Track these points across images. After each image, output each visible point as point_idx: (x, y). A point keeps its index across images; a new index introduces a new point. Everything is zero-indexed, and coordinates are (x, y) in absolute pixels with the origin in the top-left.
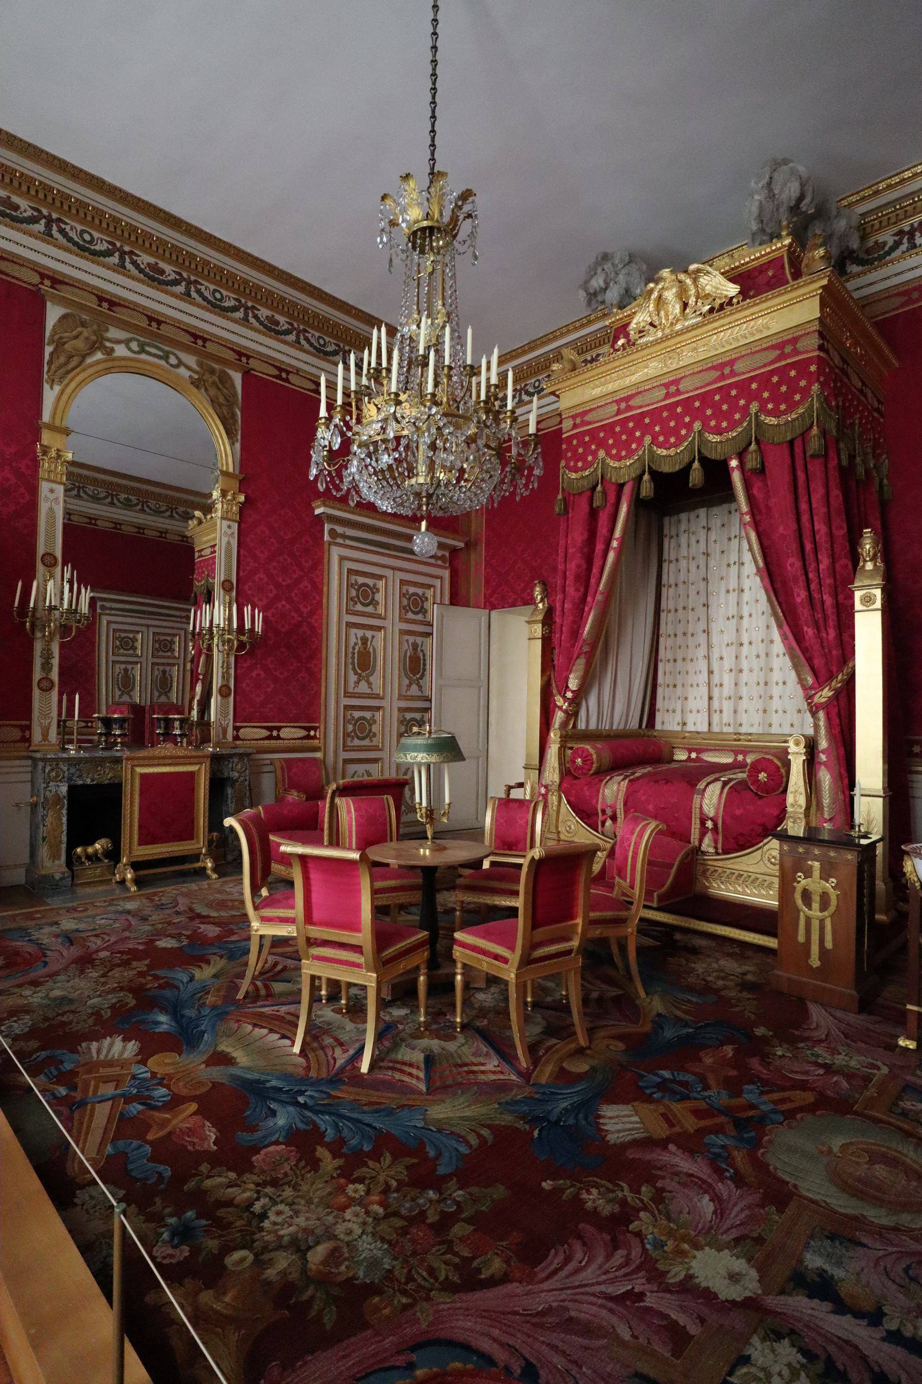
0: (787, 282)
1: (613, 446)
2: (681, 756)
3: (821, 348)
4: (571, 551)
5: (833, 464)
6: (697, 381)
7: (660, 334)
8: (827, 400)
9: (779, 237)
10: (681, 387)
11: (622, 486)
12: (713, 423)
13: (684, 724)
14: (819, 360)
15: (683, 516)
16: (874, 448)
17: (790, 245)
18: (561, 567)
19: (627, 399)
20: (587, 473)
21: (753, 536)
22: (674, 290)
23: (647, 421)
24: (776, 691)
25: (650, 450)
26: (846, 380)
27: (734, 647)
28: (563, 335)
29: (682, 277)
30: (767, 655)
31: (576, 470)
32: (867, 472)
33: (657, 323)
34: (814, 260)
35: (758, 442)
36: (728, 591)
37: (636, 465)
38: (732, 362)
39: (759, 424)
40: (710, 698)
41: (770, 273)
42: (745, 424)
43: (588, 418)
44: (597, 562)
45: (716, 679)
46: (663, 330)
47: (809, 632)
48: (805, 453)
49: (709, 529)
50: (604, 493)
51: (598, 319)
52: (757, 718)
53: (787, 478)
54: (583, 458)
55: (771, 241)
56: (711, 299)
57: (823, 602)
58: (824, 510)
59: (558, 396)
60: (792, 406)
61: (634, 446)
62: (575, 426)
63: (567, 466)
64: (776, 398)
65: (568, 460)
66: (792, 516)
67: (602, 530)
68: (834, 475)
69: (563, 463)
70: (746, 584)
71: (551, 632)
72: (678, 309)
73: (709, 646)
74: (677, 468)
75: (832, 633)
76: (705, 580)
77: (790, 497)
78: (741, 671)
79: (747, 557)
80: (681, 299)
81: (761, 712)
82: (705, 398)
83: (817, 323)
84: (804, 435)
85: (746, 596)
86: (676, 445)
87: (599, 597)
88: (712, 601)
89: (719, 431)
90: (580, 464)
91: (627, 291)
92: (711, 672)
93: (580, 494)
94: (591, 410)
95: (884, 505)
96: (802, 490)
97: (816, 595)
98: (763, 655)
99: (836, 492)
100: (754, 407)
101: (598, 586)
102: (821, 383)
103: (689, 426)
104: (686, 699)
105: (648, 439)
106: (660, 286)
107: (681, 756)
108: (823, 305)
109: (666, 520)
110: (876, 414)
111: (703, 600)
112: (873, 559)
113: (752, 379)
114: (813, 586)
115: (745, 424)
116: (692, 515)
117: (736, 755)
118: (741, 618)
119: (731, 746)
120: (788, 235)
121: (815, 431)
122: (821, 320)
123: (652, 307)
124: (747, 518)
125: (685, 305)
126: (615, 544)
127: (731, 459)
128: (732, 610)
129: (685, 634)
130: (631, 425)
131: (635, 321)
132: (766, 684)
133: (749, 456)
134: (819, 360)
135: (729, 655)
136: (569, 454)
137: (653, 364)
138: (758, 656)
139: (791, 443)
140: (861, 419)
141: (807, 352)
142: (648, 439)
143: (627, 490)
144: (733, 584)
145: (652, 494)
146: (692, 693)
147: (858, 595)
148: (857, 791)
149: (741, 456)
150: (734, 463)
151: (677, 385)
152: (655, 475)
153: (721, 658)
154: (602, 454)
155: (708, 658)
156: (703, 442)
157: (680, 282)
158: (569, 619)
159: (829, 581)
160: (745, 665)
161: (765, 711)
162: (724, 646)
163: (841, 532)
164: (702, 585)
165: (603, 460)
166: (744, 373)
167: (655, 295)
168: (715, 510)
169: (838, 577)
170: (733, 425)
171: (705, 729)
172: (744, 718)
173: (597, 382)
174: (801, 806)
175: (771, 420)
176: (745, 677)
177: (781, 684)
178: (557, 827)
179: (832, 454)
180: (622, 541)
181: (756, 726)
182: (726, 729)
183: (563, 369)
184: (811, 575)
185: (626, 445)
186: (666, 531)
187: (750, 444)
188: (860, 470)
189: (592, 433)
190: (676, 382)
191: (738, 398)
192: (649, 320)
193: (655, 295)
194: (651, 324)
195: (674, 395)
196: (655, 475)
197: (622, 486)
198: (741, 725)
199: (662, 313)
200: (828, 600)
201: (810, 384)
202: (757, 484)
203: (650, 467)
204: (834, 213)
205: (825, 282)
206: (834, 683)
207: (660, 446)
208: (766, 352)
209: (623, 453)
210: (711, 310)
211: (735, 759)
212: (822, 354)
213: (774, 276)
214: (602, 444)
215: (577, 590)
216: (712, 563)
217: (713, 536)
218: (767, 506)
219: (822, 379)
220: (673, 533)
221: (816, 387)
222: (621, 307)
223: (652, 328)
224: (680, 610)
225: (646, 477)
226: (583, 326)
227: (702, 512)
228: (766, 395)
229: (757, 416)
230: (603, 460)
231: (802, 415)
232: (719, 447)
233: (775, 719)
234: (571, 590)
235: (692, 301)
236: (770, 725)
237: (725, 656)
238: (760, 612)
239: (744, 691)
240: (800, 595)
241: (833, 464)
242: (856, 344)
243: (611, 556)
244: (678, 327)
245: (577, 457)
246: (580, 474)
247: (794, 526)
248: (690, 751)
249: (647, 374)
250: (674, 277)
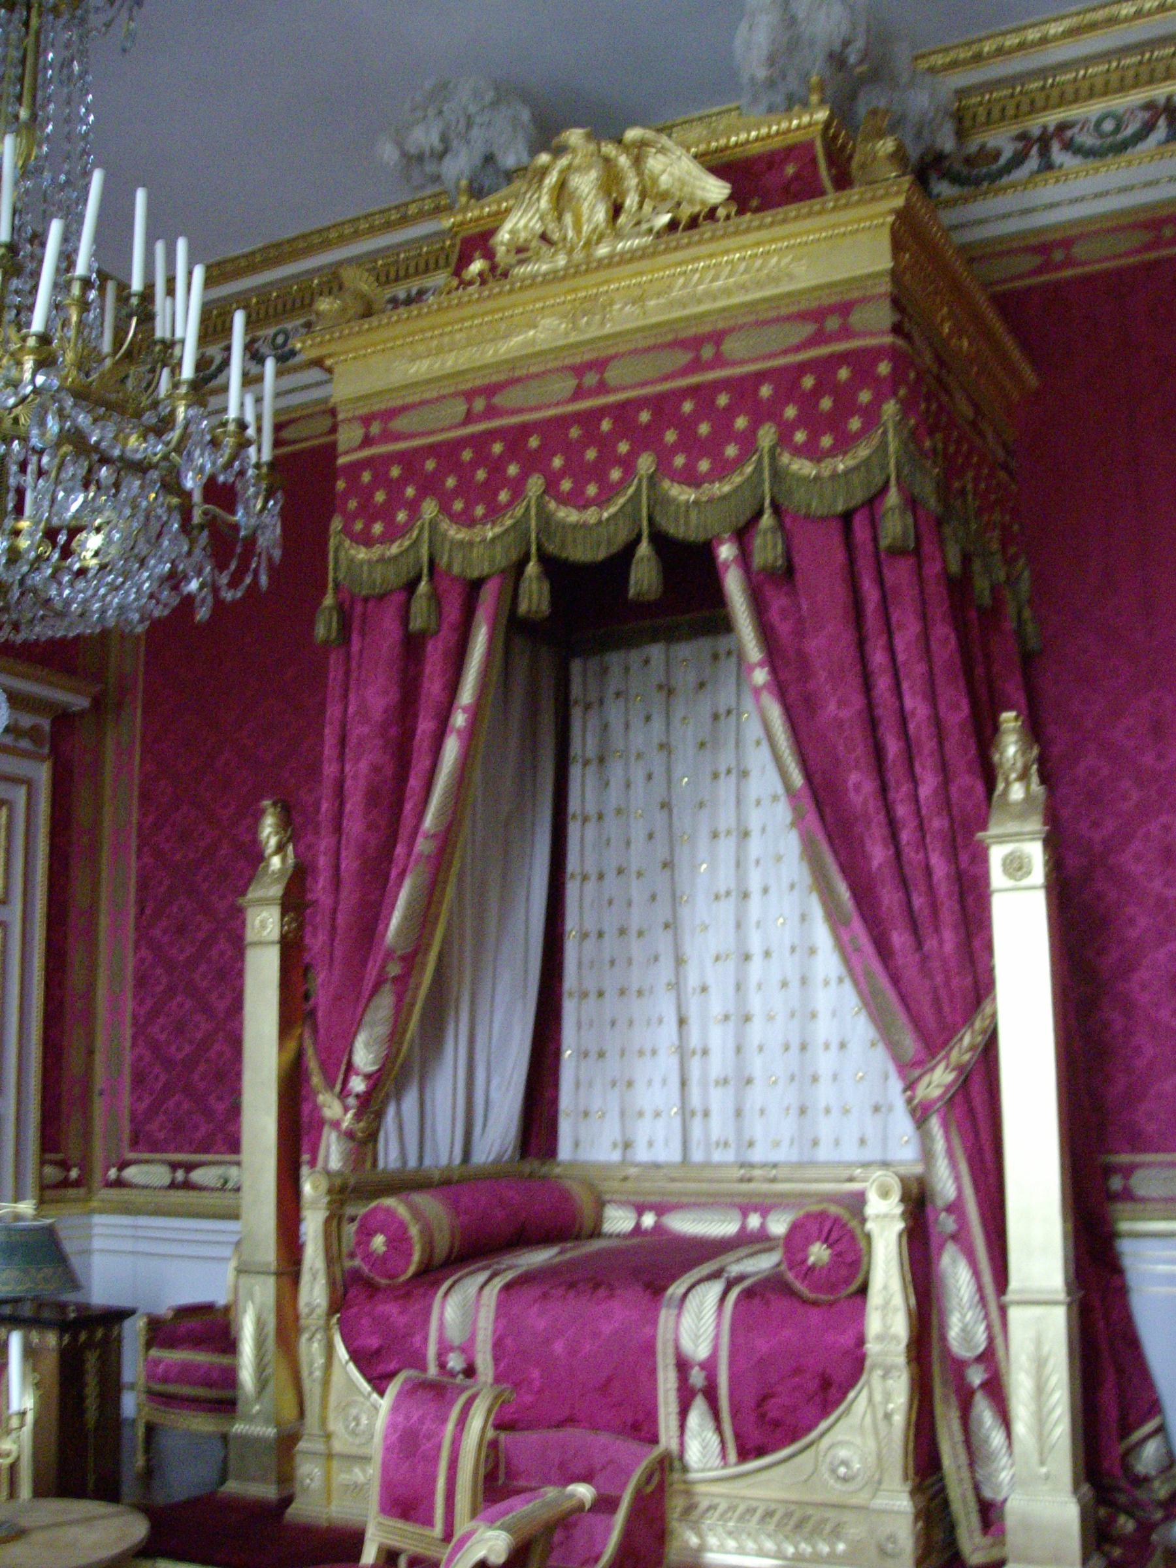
0: (822, 193)
2: (618, 1221)
3: (897, 329)
4: (358, 731)
5: (933, 569)
6: (647, 368)
7: (562, 261)
8: (914, 436)
9: (805, 104)
10: (612, 375)
11: (475, 586)
12: (679, 461)
13: (627, 1145)
14: (893, 354)
15: (615, 659)
16: (1004, 545)
17: (827, 125)
18: (330, 770)
19: (491, 390)
20: (395, 549)
21: (775, 712)
22: (593, 174)
23: (534, 442)
24: (825, 1063)
25: (541, 507)
26: (945, 399)
27: (730, 965)
28: (343, 240)
29: (609, 149)
30: (804, 981)
31: (366, 540)
32: (995, 589)
33: (556, 236)
34: (874, 158)
35: (777, 509)
36: (715, 835)
37: (510, 538)
38: (718, 338)
39: (777, 474)
40: (684, 1083)
41: (790, 170)
42: (749, 469)
43: (400, 424)
44: (420, 764)
45: (694, 1040)
46: (570, 252)
47: (899, 939)
48: (875, 539)
49: (670, 692)
50: (436, 597)
51: (422, 215)
52: (787, 1127)
53: (841, 590)
54: (386, 513)
55: (789, 109)
56: (669, 204)
57: (928, 871)
58: (920, 668)
59: (329, 370)
60: (844, 443)
61: (503, 496)
62: (367, 441)
63: (347, 531)
64: (810, 420)
65: (350, 518)
66: (853, 680)
67: (433, 687)
68: (936, 591)
69: (337, 524)
70: (755, 819)
71: (301, 927)
72: (601, 214)
73: (679, 961)
74: (601, 555)
75: (950, 939)
76: (666, 806)
77: (848, 637)
78: (747, 1018)
79: (759, 760)
80: (608, 194)
81: (794, 1111)
82: (663, 405)
83: (887, 279)
84: (873, 501)
85: (755, 846)
86: (601, 501)
87: (423, 846)
88: (683, 856)
89: (691, 478)
90: (377, 528)
91: (489, 159)
92: (682, 1022)
93: (381, 598)
94: (405, 408)
95: (1028, 660)
96: (872, 621)
97: (911, 854)
98: (795, 984)
99: (942, 631)
100: (767, 436)
101: (420, 815)
102: (902, 402)
103: (628, 464)
104: (630, 1084)
105: (535, 484)
106: (564, 162)
107: (618, 1221)
108: (897, 246)
109: (576, 666)
110: (1002, 475)
111: (662, 853)
112: (1024, 776)
113: (760, 377)
114: (905, 836)
115: (749, 469)
116: (635, 657)
118: (746, 896)
119: (732, 1195)
120: (822, 102)
121: (893, 498)
122: (895, 275)
123: (544, 203)
124: (760, 676)
125: (617, 210)
126: (459, 720)
127: (721, 543)
128: (725, 878)
129: (622, 932)
130: (498, 448)
131: (508, 226)
132: (803, 1047)
133: (758, 542)
134: (893, 354)
135: (720, 979)
136: (352, 504)
137: (548, 322)
138: (784, 984)
139: (846, 518)
140: (976, 480)
141: (872, 334)
142: (535, 484)
143: (487, 596)
144: (726, 818)
145: (545, 607)
146: (643, 1070)
147: (997, 855)
148: (1010, 1296)
149: (743, 535)
150: (726, 552)
152: (553, 566)
153: (704, 989)
154: (429, 508)
155: (676, 986)
156: (658, 501)
157: (607, 160)
158: (349, 897)
159: (937, 824)
160: (756, 1004)
161: (803, 1111)
162: (709, 962)
163: (957, 714)
164: (660, 817)
165: (433, 525)
166: (742, 362)
167: (552, 179)
168: (684, 650)
169: (955, 811)
170: (723, 469)
171: (676, 1156)
172: (757, 1128)
173: (421, 348)
174: (895, 1338)
175: (803, 467)
176: (756, 1031)
177: (834, 1046)
178: (323, 1421)
179: (928, 548)
180: (475, 714)
181: (785, 1144)
182: (717, 1156)
183: (344, 310)
184: (902, 811)
185: (488, 493)
186: (576, 690)
187: (759, 513)
188: (982, 585)
189: (408, 459)
190: (600, 365)
191: (731, 412)
192: (538, 227)
193: (552, 179)
194: (544, 237)
196: (553, 566)
197: (475, 586)
198: (751, 1144)
199: (568, 219)
200: (940, 867)
201: (877, 402)
202: (778, 602)
203: (539, 549)
204: (904, 79)
205: (899, 202)
206: (954, 1055)
207: (565, 500)
208: (787, 326)
209: (480, 511)
210: (673, 226)
212: (900, 342)
213: (796, 177)
214: (429, 486)
215: (371, 826)
216: (679, 769)
217: (679, 711)
218: (800, 653)
219: (902, 392)
220: (593, 696)
221: (890, 408)
222: (477, 192)
223: (545, 248)
224: (611, 876)
225: (532, 568)
226: (389, 226)
227: (656, 651)
228: (791, 412)
229: (773, 458)
230: (433, 525)
231: (866, 462)
232: (693, 515)
233: (825, 1128)
234: (354, 826)
235: (631, 201)
236: (815, 1143)
237: (711, 981)
238: (785, 884)
239: (757, 1066)
240: (878, 854)
241: (933, 569)
242: (958, 331)
243: (451, 749)
244: (603, 251)
245: (369, 513)
246: (377, 551)
247: (857, 701)
248: (640, 1210)
249: (533, 341)
250: (592, 147)
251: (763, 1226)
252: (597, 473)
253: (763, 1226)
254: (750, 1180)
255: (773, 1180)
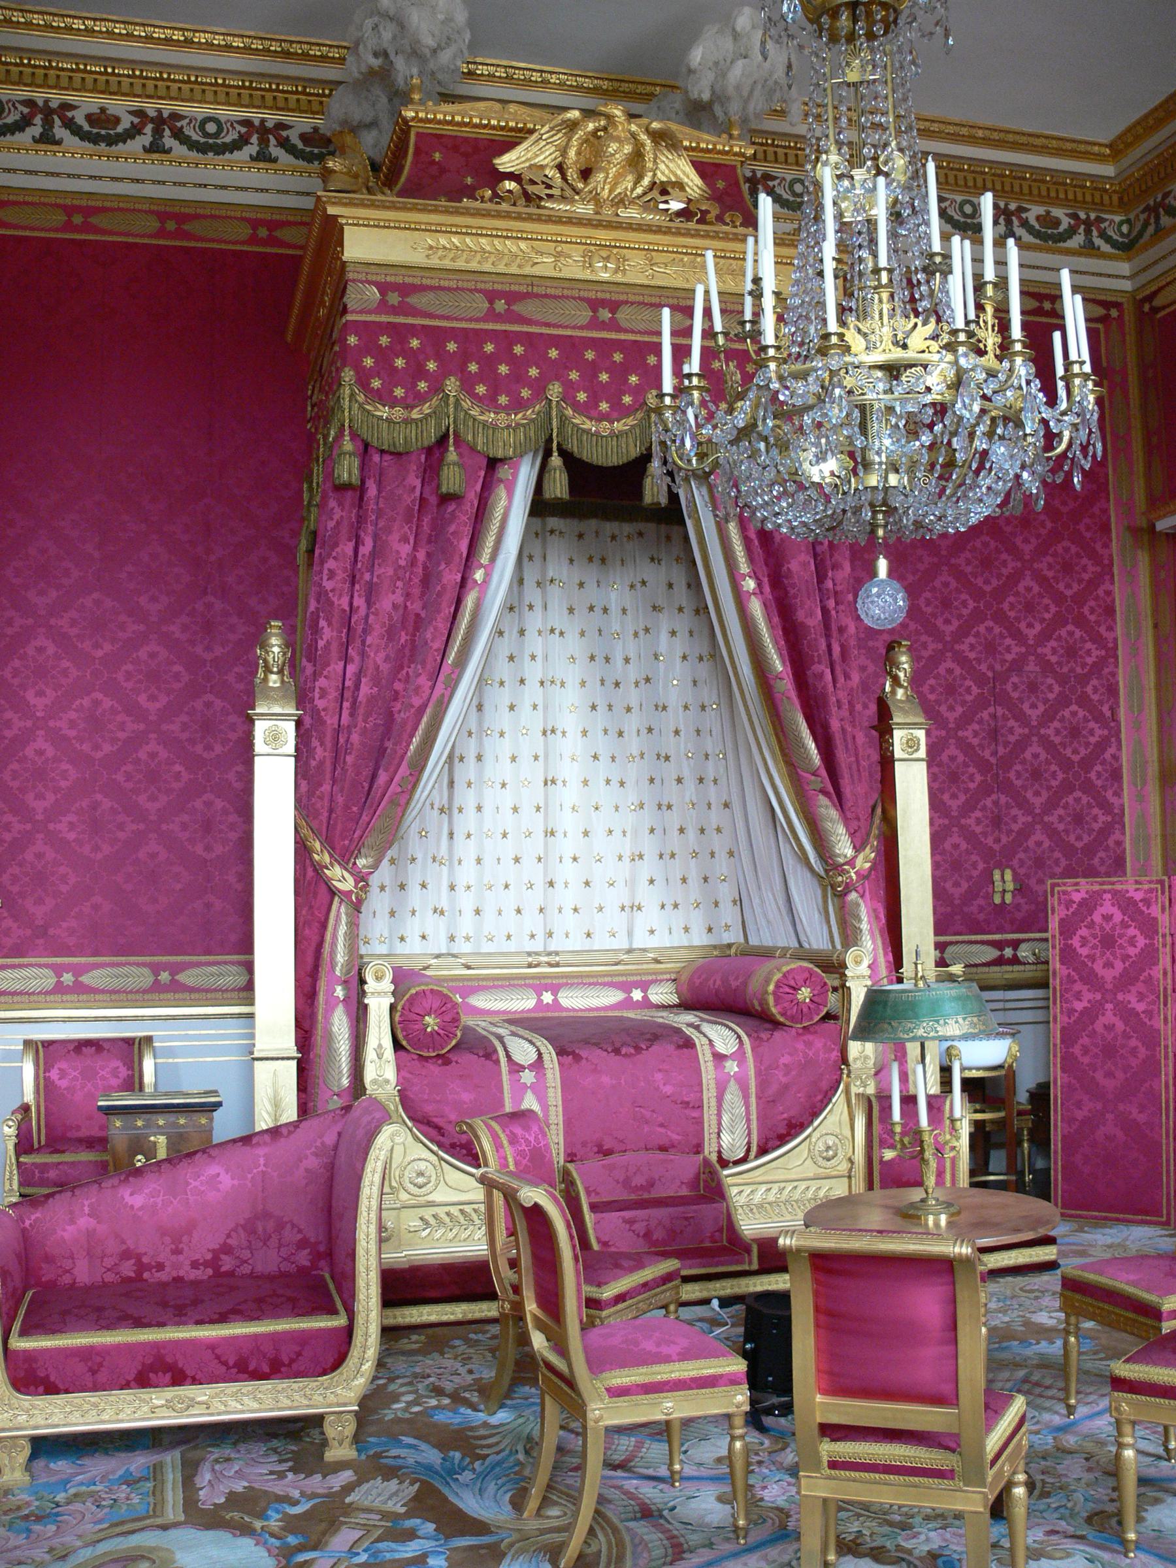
1: (480, 378)
69: (348, 375)
74: (614, 460)
105: (555, 390)
117: (539, 995)
151: (613, 311)
154: (452, 385)
195: (603, 326)
211: (540, 1001)
246: (398, 413)
251: (556, 1001)
252: (613, 394)
253: (556, 1001)
254: (536, 966)
255: (557, 965)
